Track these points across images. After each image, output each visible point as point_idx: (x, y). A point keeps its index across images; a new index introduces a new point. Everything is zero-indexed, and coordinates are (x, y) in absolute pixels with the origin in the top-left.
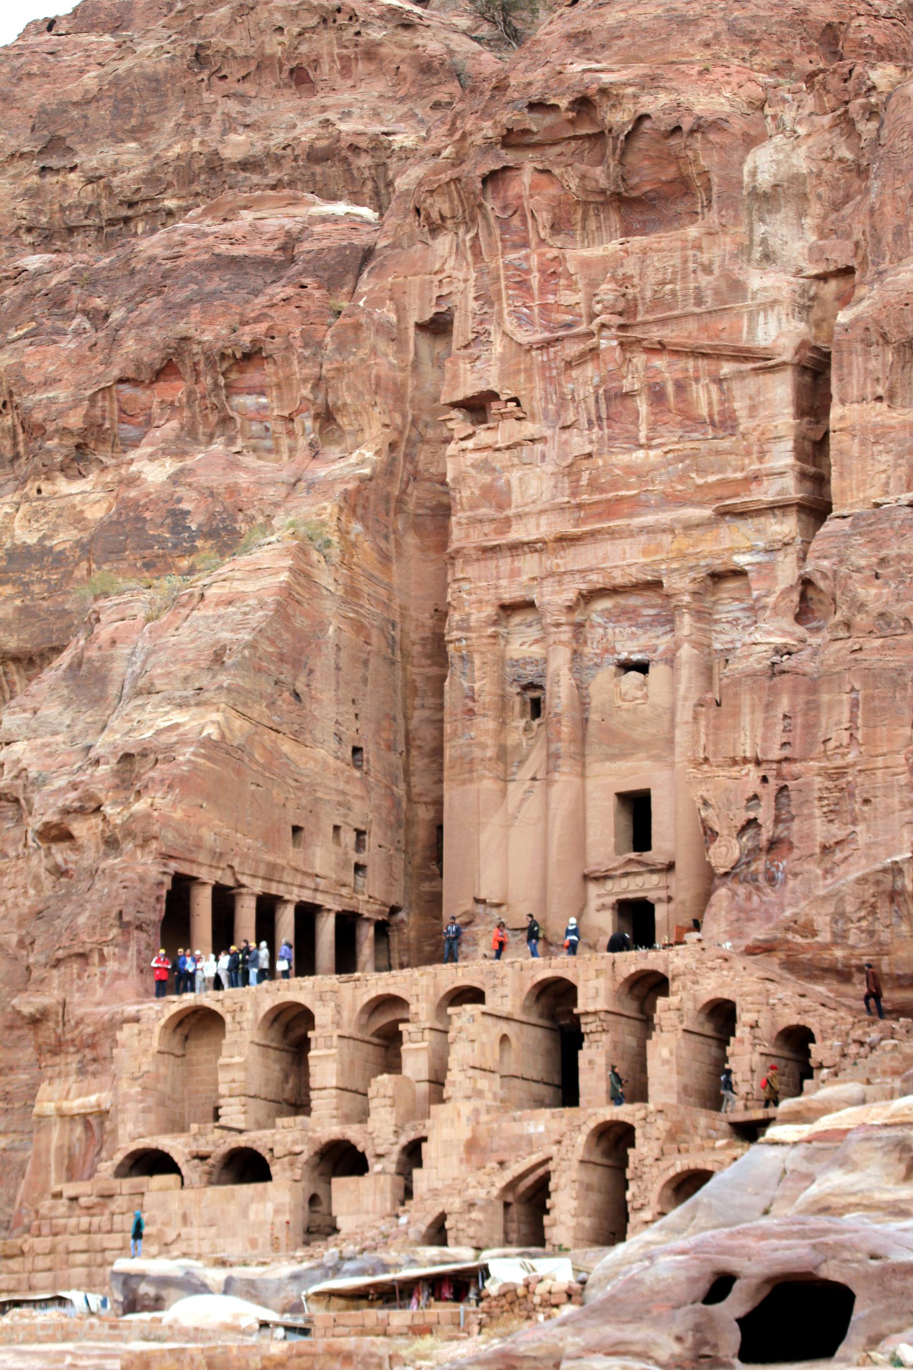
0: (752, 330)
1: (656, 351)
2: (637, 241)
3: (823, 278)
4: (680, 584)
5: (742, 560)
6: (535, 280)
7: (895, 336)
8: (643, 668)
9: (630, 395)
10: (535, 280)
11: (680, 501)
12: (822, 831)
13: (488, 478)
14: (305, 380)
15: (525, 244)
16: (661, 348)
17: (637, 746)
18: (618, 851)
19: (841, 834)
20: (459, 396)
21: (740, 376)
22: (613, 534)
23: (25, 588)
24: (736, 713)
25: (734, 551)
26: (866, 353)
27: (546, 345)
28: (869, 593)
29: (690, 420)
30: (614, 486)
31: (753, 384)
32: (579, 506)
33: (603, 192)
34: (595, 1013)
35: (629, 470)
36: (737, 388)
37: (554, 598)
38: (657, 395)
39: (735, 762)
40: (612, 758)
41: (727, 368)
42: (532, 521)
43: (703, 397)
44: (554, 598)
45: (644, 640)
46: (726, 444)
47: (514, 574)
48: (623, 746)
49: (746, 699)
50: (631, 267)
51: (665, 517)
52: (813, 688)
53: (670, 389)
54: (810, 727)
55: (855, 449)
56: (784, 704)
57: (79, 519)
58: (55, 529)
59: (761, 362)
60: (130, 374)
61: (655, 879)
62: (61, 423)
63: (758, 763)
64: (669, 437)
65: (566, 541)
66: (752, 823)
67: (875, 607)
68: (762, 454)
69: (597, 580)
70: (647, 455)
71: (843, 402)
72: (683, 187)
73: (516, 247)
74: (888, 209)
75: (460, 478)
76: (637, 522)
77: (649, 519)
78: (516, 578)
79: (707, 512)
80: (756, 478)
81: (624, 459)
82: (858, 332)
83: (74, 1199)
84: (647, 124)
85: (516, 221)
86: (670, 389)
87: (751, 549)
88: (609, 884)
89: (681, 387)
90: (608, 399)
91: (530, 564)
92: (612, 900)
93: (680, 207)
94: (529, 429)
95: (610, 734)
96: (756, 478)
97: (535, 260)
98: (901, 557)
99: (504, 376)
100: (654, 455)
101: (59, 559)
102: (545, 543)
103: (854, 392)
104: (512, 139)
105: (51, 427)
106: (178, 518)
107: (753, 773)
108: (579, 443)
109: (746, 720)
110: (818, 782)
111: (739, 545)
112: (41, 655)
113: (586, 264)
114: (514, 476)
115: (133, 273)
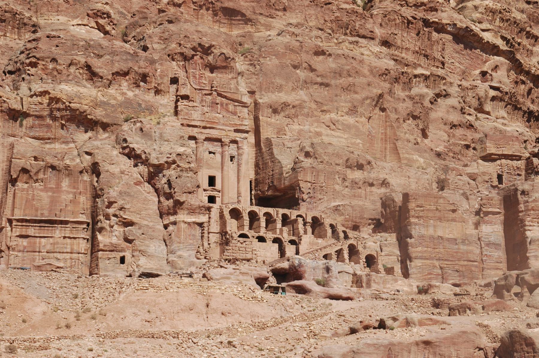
0: (241, 98)
1: (223, 98)
2: (219, 75)
3: (248, 92)
4: (226, 140)
5: (238, 139)
6: (197, 76)
7: (273, 106)
8: (214, 153)
9: (217, 104)
10: (197, 76)
11: (226, 125)
12: (320, 197)
13: (187, 111)
14: (156, 83)
15: (196, 69)
16: (225, 97)
17: (213, 168)
18: (209, 186)
19: (322, 197)
20: (181, 94)
21: (239, 106)
22: (213, 128)
23: (106, 110)
24: (307, 173)
25: (237, 137)
26: (267, 109)
27: (200, 90)
28: (325, 157)
29: (227, 111)
30: (213, 119)
31: (240, 108)
32: (207, 121)
33: (211, 64)
34: (309, 223)
35: (215, 117)
36: (238, 107)
37: (201, 137)
38: (222, 105)
39: (306, 181)
40: (208, 169)
41: (236, 104)
42: (196, 122)
43: (231, 108)
44: (201, 137)
45: (215, 148)
46: (234, 117)
47: (192, 131)
48: (210, 167)
49: (309, 171)
50: (218, 79)
51: (224, 128)
52: (318, 172)
53: (224, 105)
54: (318, 178)
55: (265, 125)
56: (314, 174)
57: (115, 99)
58: (110, 100)
59: (244, 105)
60: (119, 70)
61: (217, 192)
62: (107, 77)
63: (309, 182)
64: (225, 114)
65: (205, 128)
66: (309, 193)
67: (326, 160)
68: (242, 121)
69: (210, 136)
70: (218, 116)
71: (262, 116)
72: (225, 67)
73: (193, 69)
74: (264, 83)
75: (182, 110)
76: (218, 127)
77: (221, 127)
78: (194, 132)
79: (232, 129)
80: (241, 125)
81: (215, 115)
82: (267, 105)
83: (239, 241)
84: (223, 55)
85: (194, 65)
86: (224, 105)
87: (240, 138)
88: (208, 192)
89: (227, 105)
90: (212, 103)
91: (196, 130)
92: (208, 195)
93: (223, 71)
94: (195, 104)
95: (208, 164)
96: (241, 125)
97: (198, 73)
98: (328, 153)
99: (191, 93)
100: (221, 116)
101: (113, 106)
102: (200, 126)
103: (265, 115)
104: (194, 49)
105: (104, 78)
106: (140, 105)
107: (309, 184)
108: (206, 109)
109: (309, 175)
110: (319, 188)
111: (238, 136)
112: (112, 125)
113: (209, 77)
114: (193, 112)
115: (102, 48)
